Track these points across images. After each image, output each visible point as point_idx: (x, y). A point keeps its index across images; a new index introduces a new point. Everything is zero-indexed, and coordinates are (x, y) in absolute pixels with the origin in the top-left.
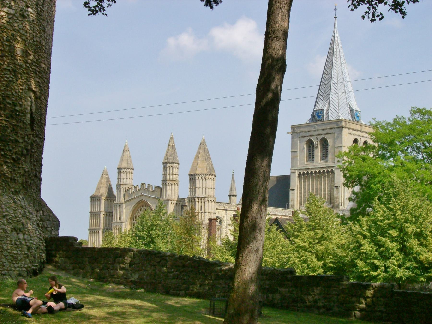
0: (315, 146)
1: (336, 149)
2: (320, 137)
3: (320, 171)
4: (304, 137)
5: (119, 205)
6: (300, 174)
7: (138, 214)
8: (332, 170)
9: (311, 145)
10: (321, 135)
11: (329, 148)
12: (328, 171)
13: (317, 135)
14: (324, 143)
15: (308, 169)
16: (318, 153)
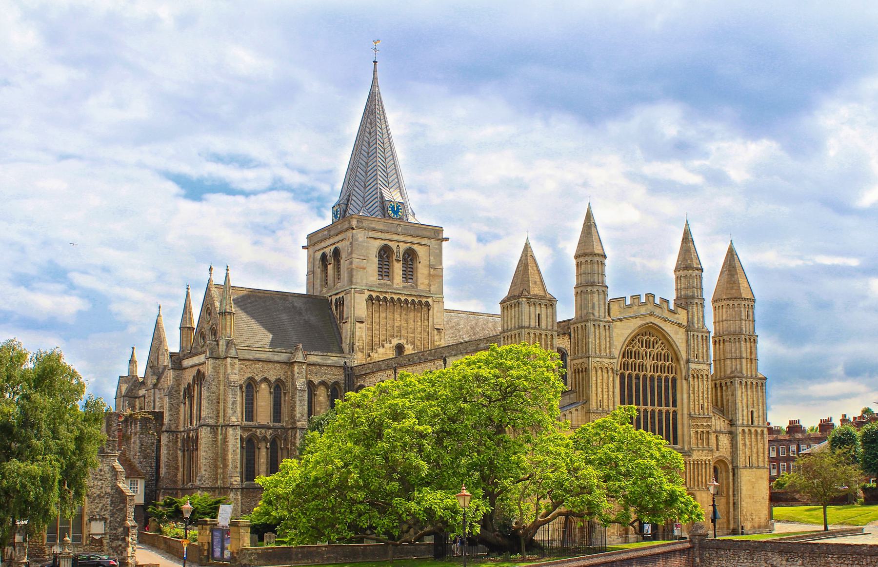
0: (394, 257)
1: (432, 270)
2: (403, 247)
3: (406, 300)
4: (375, 239)
5: (604, 324)
6: (370, 297)
7: (633, 347)
8: (427, 304)
9: (385, 253)
10: (406, 243)
11: (419, 266)
12: (420, 302)
13: (399, 242)
14: (410, 256)
15: (386, 292)
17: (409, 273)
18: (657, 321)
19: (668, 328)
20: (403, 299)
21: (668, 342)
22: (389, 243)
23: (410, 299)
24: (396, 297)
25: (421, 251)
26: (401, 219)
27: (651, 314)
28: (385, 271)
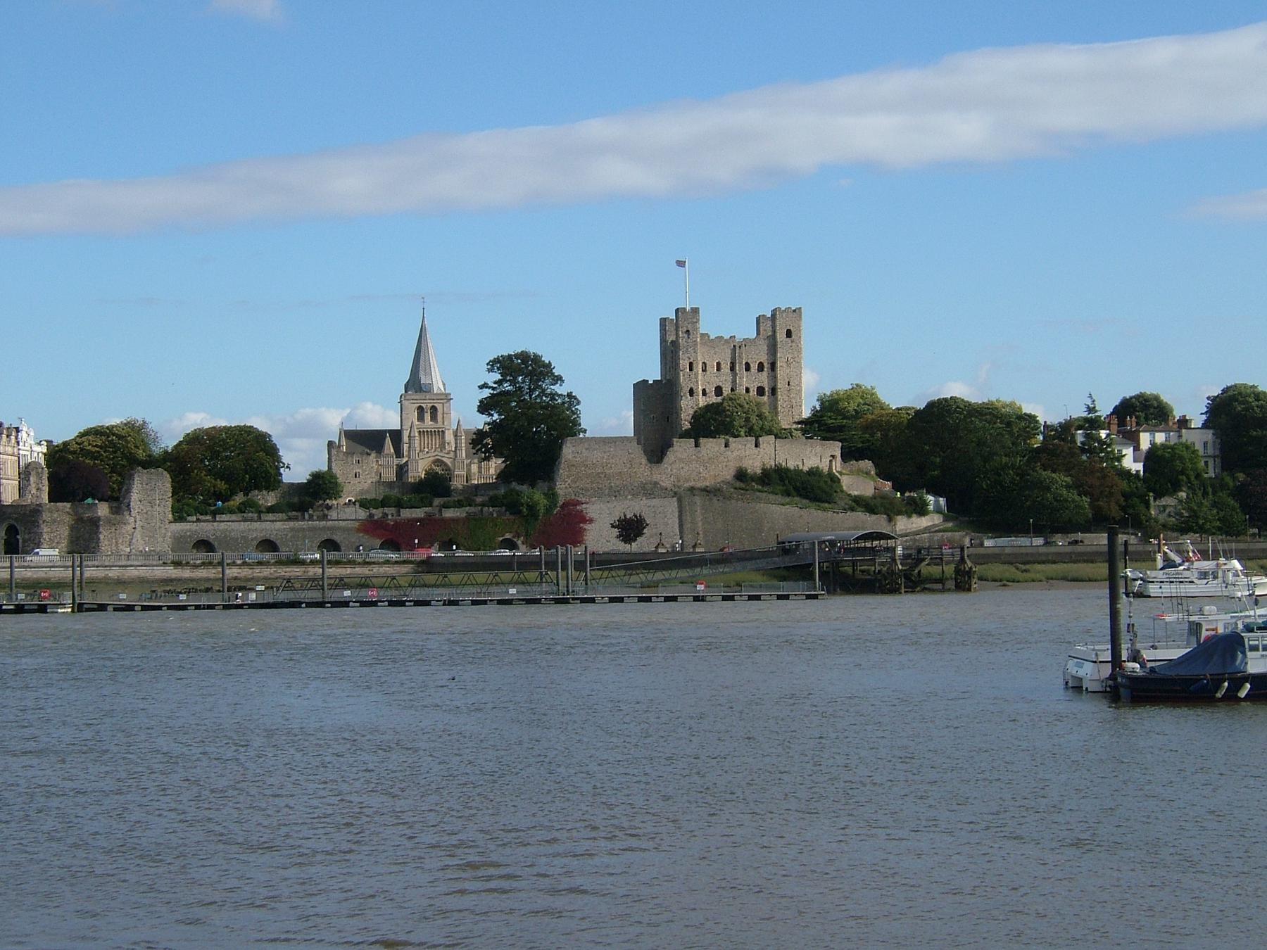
9: (421, 410)
11: (438, 413)
12: (439, 431)
14: (434, 409)
16: (428, 416)
17: (434, 418)
18: (439, 458)
19: (444, 459)
20: (429, 430)
21: (446, 464)
22: (422, 405)
23: (433, 430)
24: (425, 430)
25: (439, 407)
26: (430, 391)
27: (437, 455)
28: (421, 418)
